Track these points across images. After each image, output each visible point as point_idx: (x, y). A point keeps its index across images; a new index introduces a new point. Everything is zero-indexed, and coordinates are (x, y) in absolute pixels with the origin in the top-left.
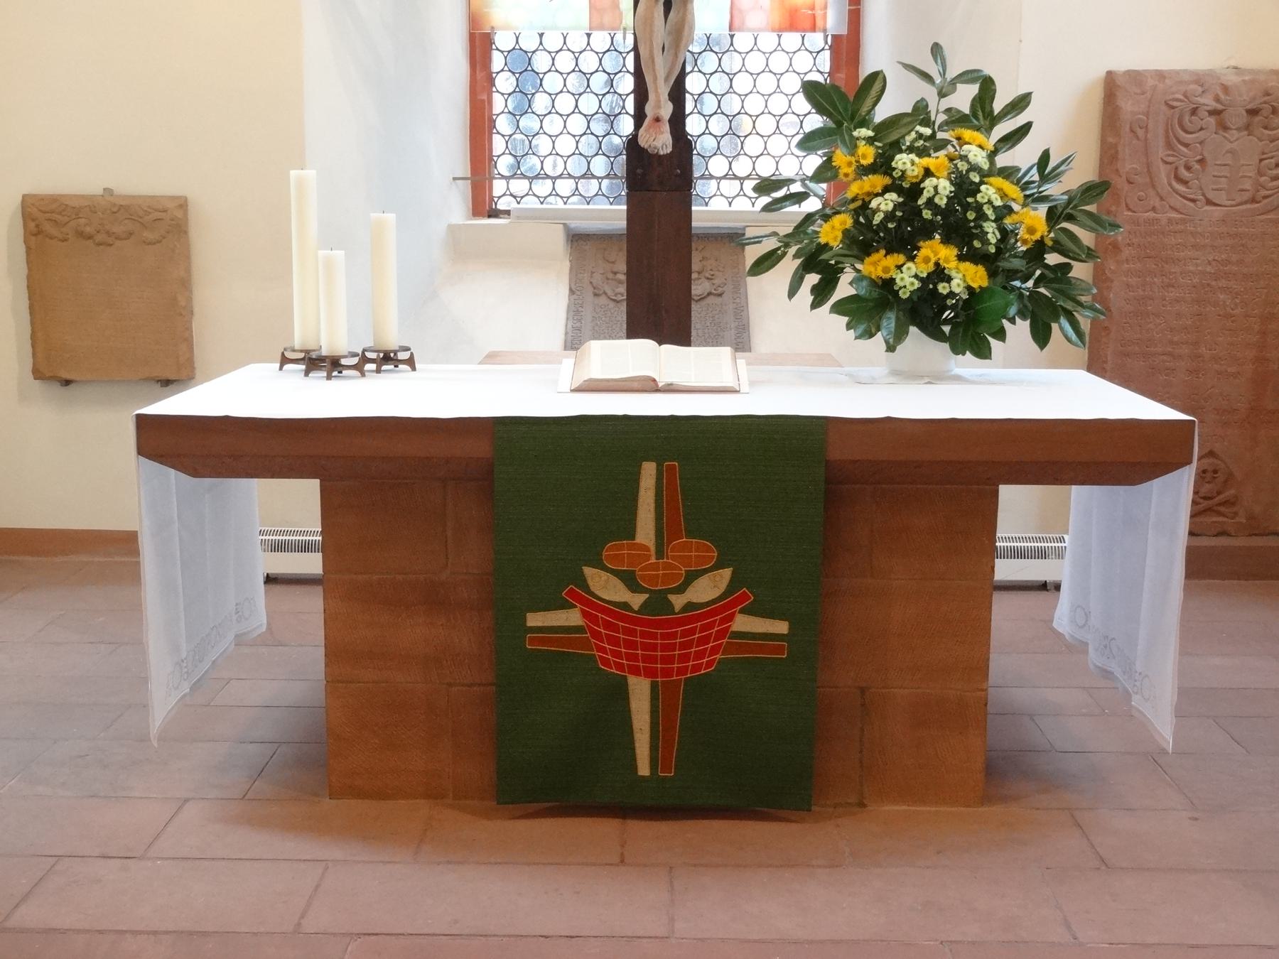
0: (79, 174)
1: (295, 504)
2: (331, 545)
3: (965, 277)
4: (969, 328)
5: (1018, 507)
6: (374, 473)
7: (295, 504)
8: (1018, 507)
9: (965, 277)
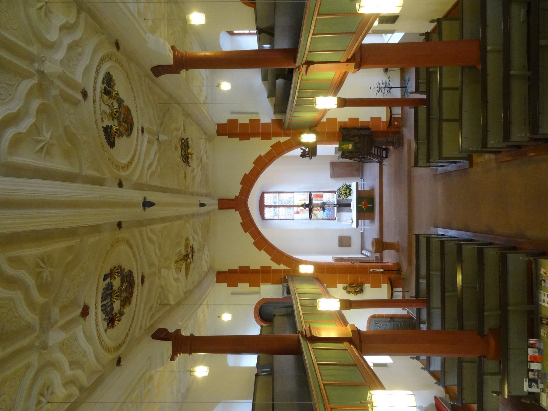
0: (337, 243)
1: (360, 221)
2: (362, 219)
3: (348, 190)
4: (350, 190)
5: (360, 189)
6: (358, 218)
7: (360, 221)
8: (360, 189)
9: (348, 190)
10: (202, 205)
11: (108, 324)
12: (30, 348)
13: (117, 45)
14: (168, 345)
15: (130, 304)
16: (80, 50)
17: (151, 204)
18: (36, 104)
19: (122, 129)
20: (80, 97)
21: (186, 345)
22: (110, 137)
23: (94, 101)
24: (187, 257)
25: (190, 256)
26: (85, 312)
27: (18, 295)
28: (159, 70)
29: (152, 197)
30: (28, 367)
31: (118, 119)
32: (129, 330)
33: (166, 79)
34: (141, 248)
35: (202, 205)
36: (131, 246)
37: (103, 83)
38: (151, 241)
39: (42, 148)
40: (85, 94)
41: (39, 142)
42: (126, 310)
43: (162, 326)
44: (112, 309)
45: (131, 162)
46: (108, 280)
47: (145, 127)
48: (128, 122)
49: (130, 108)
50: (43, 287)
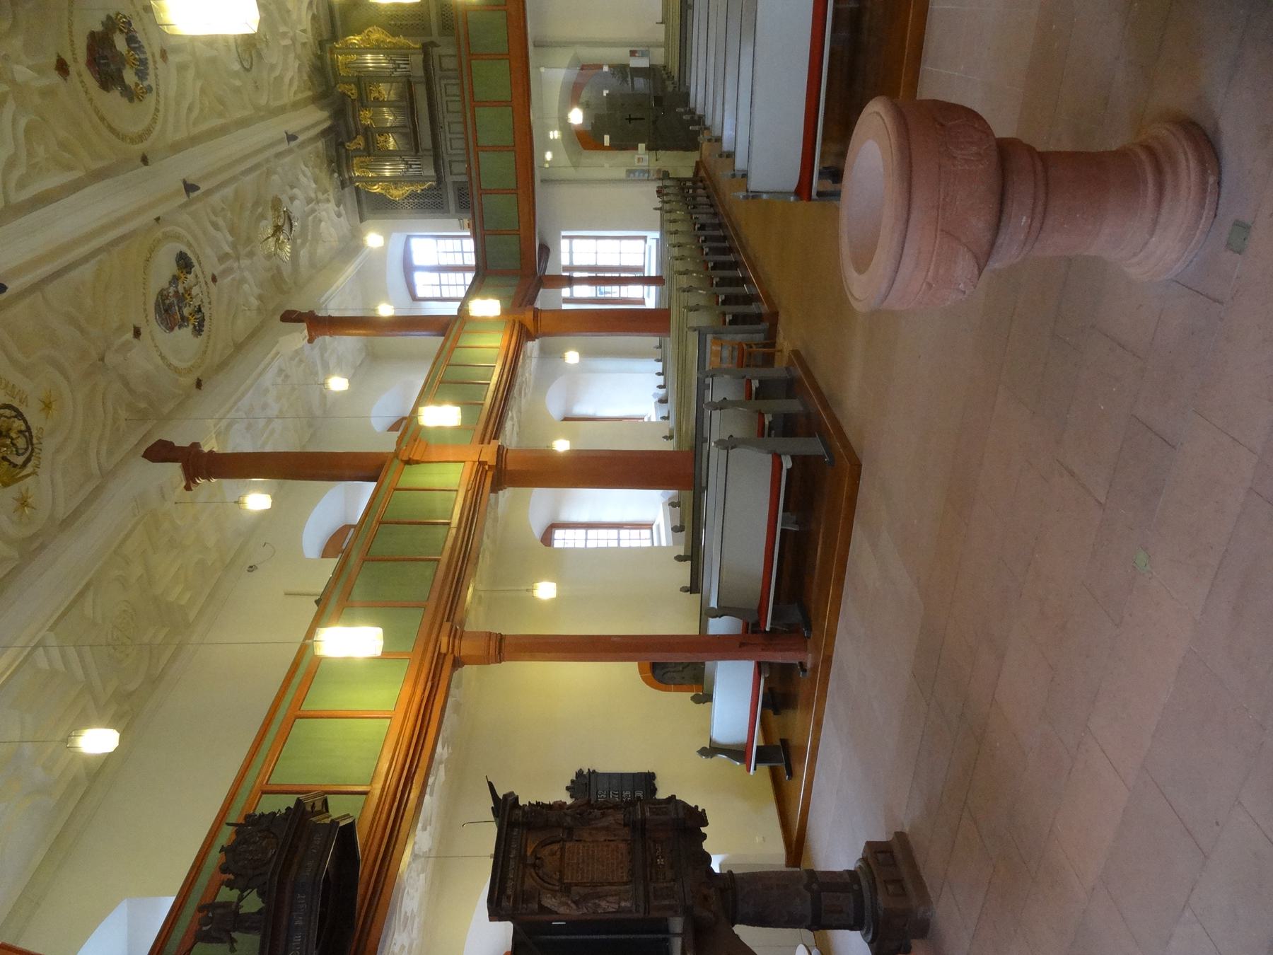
22: (184, 263)
42: (98, 28)
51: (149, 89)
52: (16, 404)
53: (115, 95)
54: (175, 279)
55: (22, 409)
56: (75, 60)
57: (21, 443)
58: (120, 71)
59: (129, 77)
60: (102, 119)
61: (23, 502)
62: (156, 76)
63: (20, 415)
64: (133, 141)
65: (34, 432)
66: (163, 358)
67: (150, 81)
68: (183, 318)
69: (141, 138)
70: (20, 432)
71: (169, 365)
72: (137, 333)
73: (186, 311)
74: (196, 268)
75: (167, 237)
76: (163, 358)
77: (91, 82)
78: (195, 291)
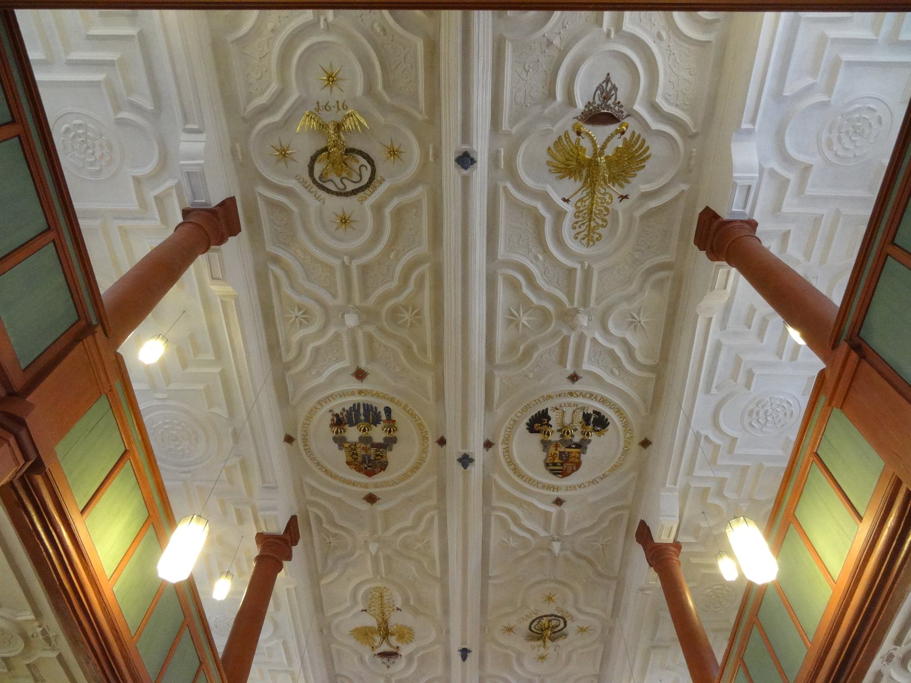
10: (465, 653)
11: (337, 415)
12: (349, 298)
13: (645, 443)
14: (278, 527)
15: (348, 463)
16: (617, 372)
17: (465, 466)
18: (549, 306)
19: (552, 450)
20: (569, 369)
21: (274, 551)
22: (538, 423)
23: (571, 394)
24: (385, 639)
25: (385, 648)
26: (360, 375)
27: (394, 284)
28: (644, 534)
29: (476, 469)
30: (335, 296)
31: (563, 441)
32: (318, 464)
33: (638, 553)
34: (411, 493)
35: (465, 653)
36: (415, 468)
37: (595, 412)
38: (419, 517)
39: (513, 315)
40: (574, 378)
41: (518, 312)
43: (300, 542)
44: (352, 425)
45: (516, 470)
46: (384, 417)
47: (565, 508)
48: (562, 465)
49: (580, 469)
50: (394, 313)
51: (388, 410)
52: (534, 617)
53: (392, 456)
54: (545, 444)
55: (540, 614)
56: (366, 486)
57: (554, 623)
58: (374, 445)
59: (378, 434)
60: (406, 476)
61: (582, 630)
62: (377, 395)
63: (541, 617)
64: (424, 451)
65: (556, 613)
66: (594, 482)
67: (380, 405)
68: (578, 446)
69: (425, 438)
70: (550, 621)
71: (604, 476)
72: (559, 502)
73: (577, 438)
74: (549, 405)
75: (507, 440)
76: (594, 482)
77: (380, 478)
78: (567, 420)
